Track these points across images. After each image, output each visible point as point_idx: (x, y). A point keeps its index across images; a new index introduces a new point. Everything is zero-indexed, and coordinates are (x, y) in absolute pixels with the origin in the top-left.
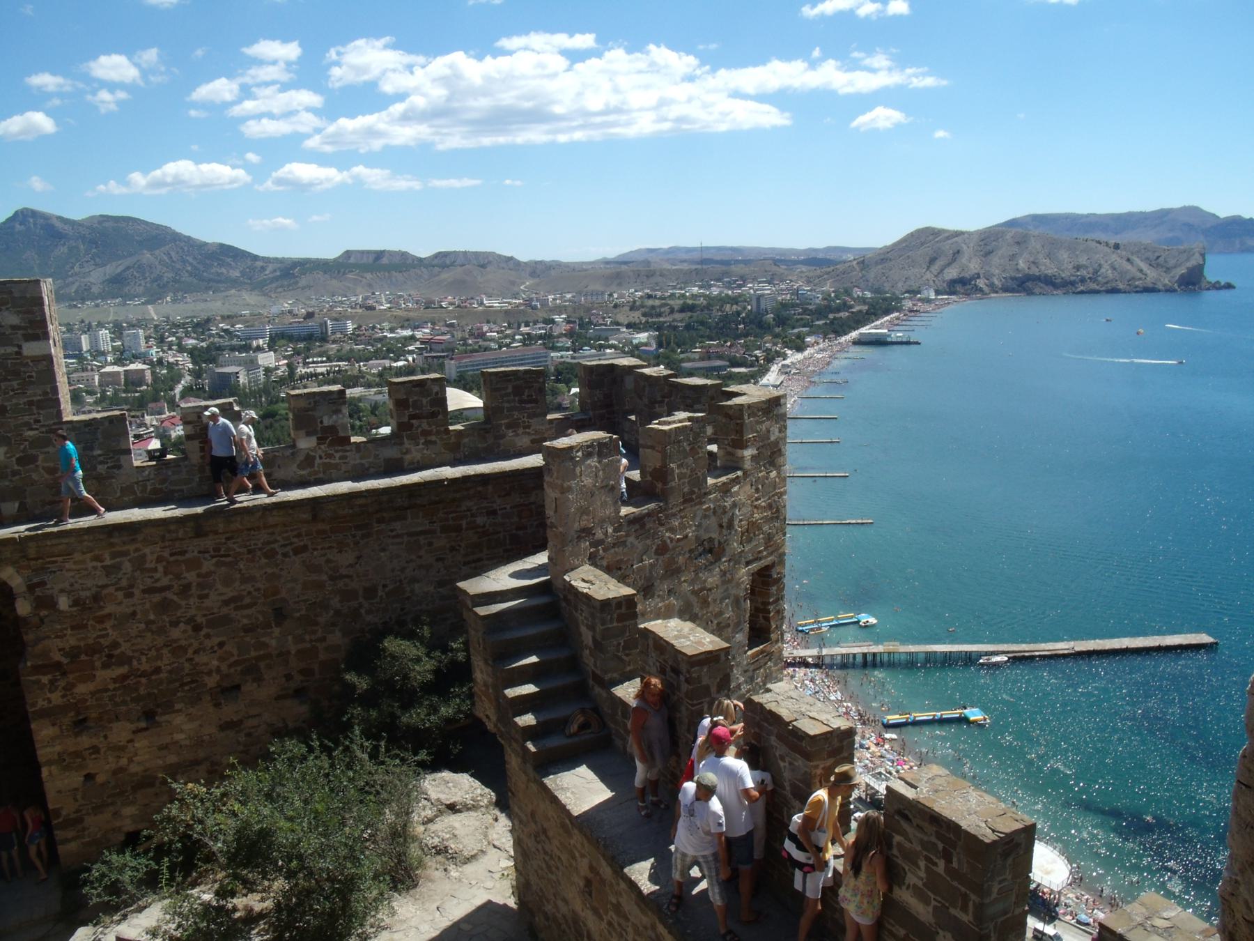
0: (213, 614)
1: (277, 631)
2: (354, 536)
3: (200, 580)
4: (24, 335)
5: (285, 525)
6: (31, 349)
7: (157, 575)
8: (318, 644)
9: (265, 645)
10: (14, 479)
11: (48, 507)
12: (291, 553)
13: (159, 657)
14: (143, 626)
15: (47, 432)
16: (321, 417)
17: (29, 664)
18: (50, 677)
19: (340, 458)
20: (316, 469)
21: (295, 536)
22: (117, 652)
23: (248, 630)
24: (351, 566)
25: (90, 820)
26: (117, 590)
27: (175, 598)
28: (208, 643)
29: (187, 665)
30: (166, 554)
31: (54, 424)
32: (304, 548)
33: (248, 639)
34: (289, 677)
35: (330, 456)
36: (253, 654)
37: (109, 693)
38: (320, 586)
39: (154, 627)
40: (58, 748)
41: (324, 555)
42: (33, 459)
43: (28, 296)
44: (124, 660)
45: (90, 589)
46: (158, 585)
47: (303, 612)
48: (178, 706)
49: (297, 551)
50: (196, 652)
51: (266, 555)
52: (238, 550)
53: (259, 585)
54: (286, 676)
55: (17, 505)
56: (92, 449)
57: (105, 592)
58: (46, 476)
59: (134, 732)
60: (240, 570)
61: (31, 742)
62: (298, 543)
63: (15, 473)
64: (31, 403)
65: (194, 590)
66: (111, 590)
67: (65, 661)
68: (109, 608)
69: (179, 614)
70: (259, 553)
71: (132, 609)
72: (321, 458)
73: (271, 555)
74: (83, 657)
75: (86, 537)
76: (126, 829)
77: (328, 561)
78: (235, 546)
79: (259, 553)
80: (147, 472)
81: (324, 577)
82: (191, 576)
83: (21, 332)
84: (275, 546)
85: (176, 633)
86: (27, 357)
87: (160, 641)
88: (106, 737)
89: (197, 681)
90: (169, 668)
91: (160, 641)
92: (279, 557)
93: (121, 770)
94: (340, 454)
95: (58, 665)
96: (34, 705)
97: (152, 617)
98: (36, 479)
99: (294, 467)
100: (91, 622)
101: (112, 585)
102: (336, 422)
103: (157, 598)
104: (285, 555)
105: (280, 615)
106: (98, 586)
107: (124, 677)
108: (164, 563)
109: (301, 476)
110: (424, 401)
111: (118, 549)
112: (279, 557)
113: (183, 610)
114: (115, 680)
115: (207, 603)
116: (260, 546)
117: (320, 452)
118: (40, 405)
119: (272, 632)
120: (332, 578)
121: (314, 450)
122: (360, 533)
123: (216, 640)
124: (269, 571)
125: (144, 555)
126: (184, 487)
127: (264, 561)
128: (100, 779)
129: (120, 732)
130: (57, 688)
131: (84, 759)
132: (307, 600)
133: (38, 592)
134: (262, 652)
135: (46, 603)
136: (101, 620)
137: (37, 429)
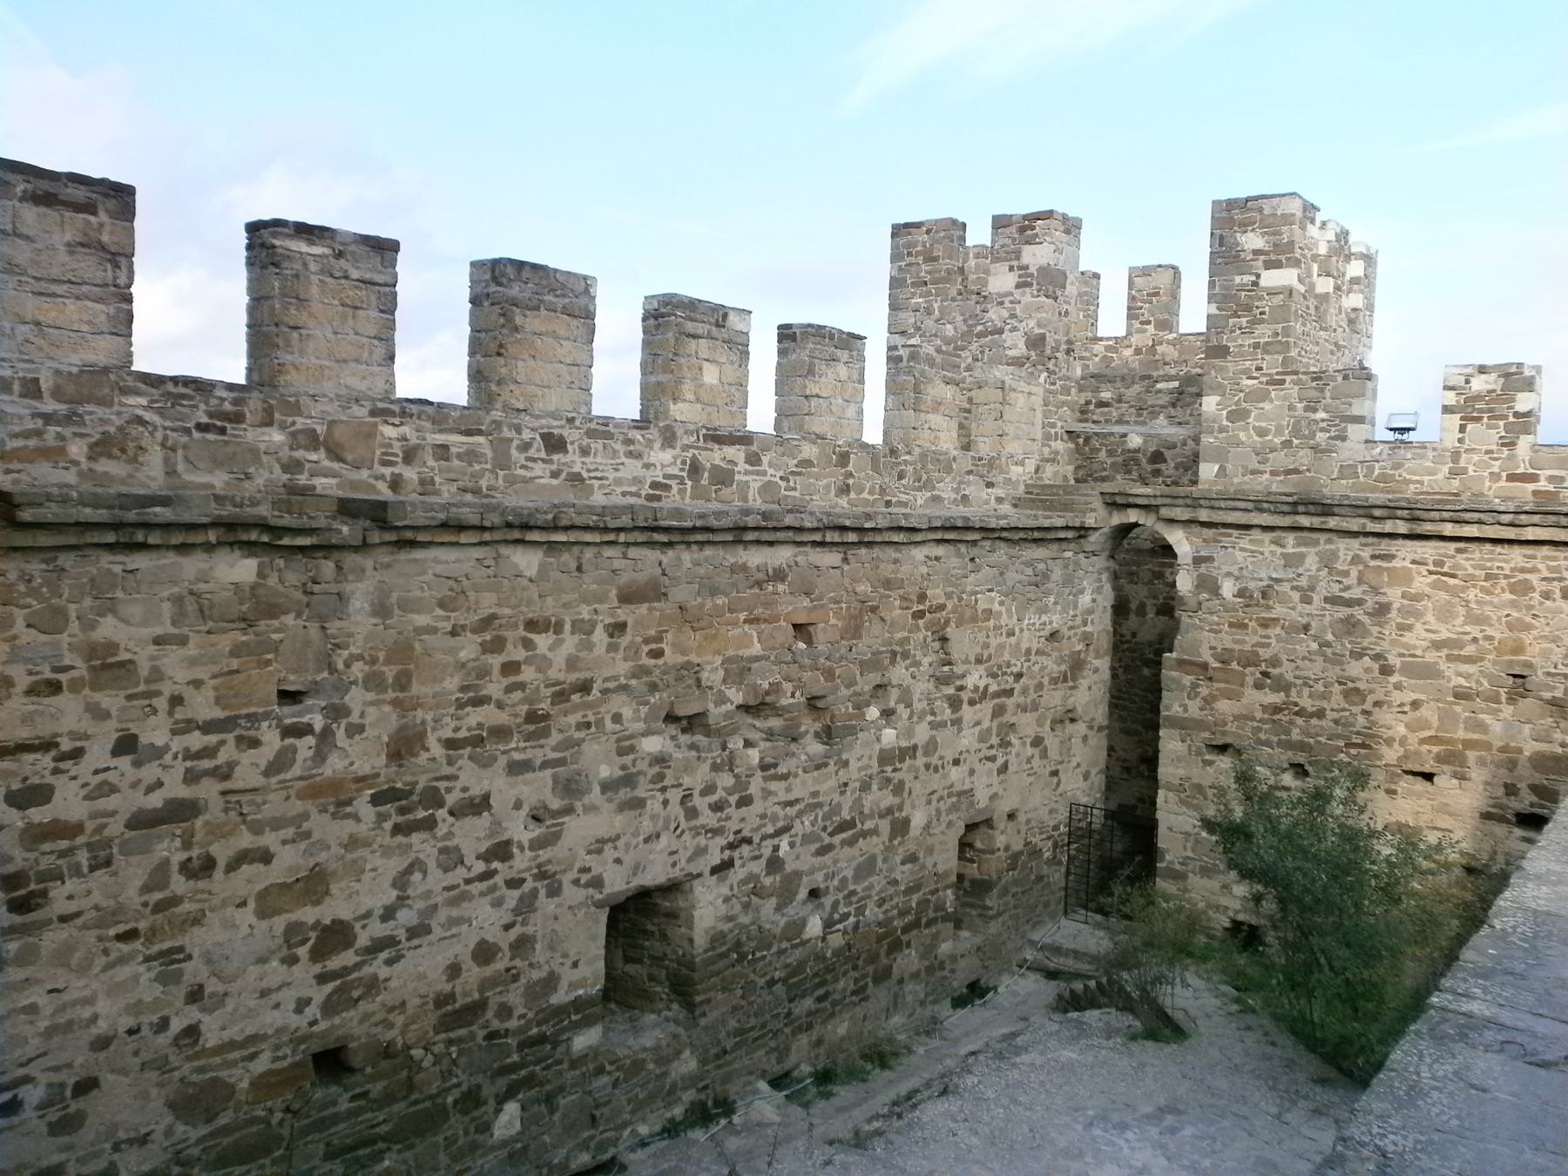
0: (1413, 656)
1: (1507, 711)
3: (1406, 602)
6: (1271, 278)
7: (1346, 581)
9: (1482, 727)
13: (1324, 696)
14: (1314, 646)
18: (1192, 678)
22: (1274, 671)
23: (1460, 695)
25: (1194, 880)
26: (1293, 588)
27: (1366, 620)
28: (1397, 697)
29: (1361, 720)
34: (1511, 790)
36: (1461, 734)
39: (1329, 651)
40: (1181, 772)
44: (1282, 686)
46: (1346, 595)
50: (1377, 704)
52: (1471, 571)
53: (1490, 632)
54: (1506, 786)
55: (1216, 467)
56: (1315, 410)
61: (1157, 751)
63: (1222, 430)
64: (1256, 346)
65: (1393, 614)
66: (1286, 587)
68: (1279, 611)
69: (1365, 644)
71: (1304, 621)
73: (1522, 588)
74: (1234, 665)
78: (1467, 564)
79: (1503, 582)
85: (1355, 668)
87: (1333, 673)
90: (1335, 715)
91: (1333, 673)
92: (1536, 595)
95: (1204, 666)
96: (1168, 708)
97: (1330, 637)
103: (1344, 612)
104: (1547, 595)
106: (1271, 579)
107: (1277, 709)
112: (1536, 595)
114: (1264, 708)
115: (1408, 638)
118: (1267, 348)
123: (1410, 696)
127: (1508, 596)
130: (1197, 694)
131: (1206, 799)
133: (1203, 569)
134: (1476, 736)
135: (1208, 585)
136: (1265, 623)
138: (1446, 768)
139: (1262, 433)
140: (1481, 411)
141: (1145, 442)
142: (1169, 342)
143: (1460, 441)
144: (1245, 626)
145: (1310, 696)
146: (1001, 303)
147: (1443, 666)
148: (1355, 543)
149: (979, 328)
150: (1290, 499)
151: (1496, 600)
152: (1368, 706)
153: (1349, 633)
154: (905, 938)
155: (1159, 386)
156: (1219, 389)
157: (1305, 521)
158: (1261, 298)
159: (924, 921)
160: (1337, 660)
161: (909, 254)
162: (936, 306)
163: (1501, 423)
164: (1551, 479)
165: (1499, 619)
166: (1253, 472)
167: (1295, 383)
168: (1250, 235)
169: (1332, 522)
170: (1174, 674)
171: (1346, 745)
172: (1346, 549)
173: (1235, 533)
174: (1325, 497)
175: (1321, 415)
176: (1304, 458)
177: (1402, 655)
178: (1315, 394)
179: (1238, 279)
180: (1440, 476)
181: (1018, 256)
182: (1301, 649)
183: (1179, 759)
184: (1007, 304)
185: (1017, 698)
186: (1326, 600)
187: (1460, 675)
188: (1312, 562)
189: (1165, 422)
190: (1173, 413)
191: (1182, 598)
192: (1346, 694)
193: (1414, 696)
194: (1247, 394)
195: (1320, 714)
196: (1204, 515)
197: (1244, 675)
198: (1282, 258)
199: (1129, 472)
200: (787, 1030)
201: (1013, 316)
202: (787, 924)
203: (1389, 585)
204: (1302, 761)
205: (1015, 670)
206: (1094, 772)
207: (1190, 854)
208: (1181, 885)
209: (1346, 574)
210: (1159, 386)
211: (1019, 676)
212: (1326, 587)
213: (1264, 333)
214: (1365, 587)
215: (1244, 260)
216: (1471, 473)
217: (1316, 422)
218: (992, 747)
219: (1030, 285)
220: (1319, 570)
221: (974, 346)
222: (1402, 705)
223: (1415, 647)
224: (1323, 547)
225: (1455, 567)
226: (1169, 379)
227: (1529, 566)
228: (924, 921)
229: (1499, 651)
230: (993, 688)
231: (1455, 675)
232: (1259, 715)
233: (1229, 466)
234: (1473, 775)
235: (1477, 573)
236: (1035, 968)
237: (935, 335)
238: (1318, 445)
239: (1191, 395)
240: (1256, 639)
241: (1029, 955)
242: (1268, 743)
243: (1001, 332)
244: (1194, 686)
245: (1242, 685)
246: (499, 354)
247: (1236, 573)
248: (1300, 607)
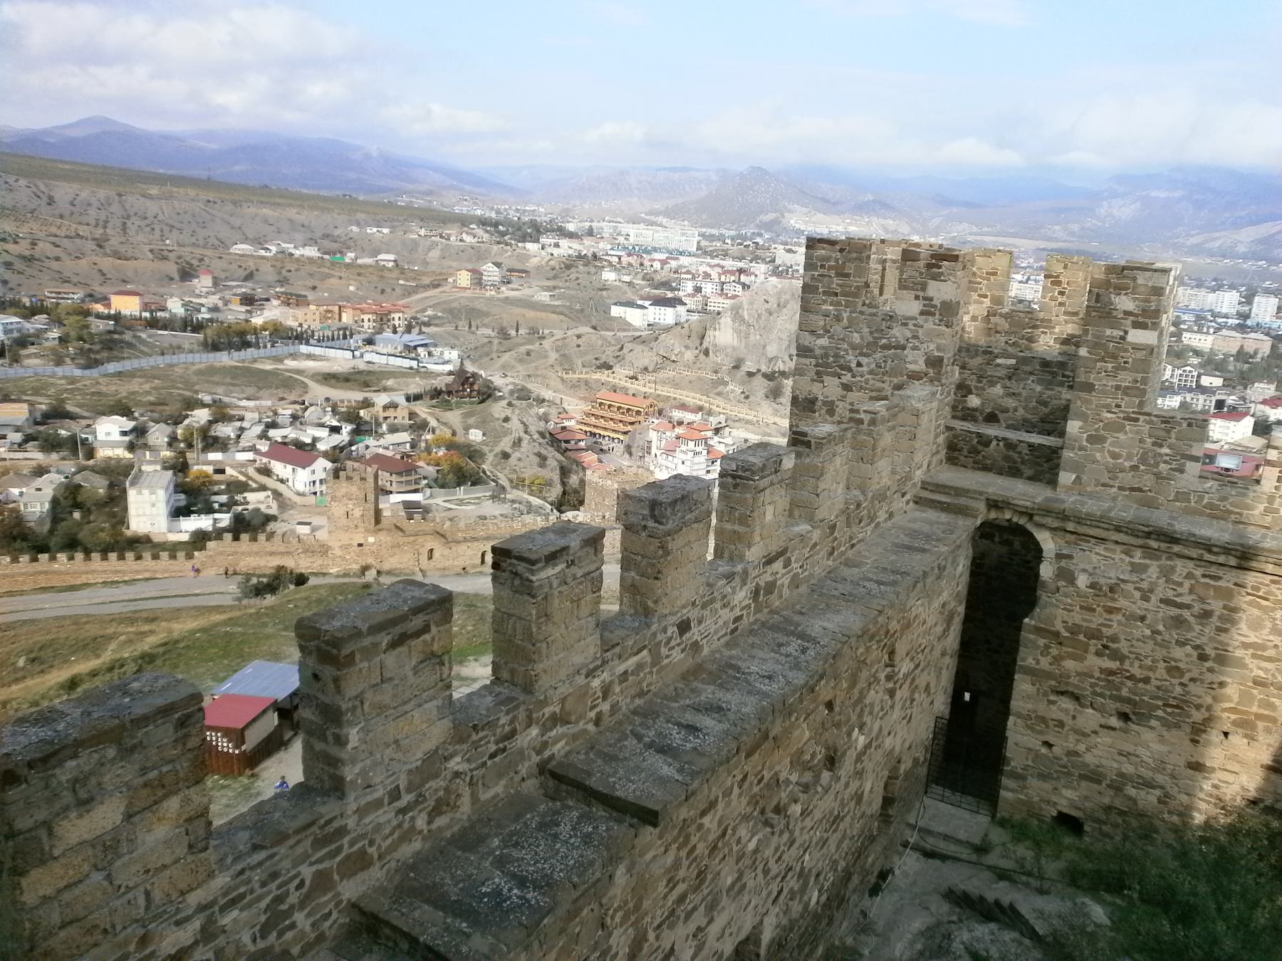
4: (1133, 322)
6: (1137, 336)
7: (1180, 590)
14: (1148, 632)
23: (1258, 683)
25: (1033, 782)
26: (1136, 589)
27: (1192, 619)
29: (1178, 689)
33: (1255, 692)
36: (1255, 709)
39: (1159, 638)
40: (1030, 706)
44: (1117, 656)
46: (1178, 600)
50: (1192, 680)
55: (1074, 476)
56: (1161, 446)
60: (1275, 619)
63: (1081, 449)
64: (1118, 388)
65: (1214, 619)
66: (1130, 587)
68: (1122, 603)
71: (1142, 613)
74: (1081, 637)
76: (1060, 808)
85: (1178, 653)
86: (1130, 344)
89: (1182, 708)
90: (1159, 683)
93: (1076, 754)
95: (1057, 634)
96: (1024, 660)
97: (1161, 628)
103: (1174, 611)
107: (1111, 672)
114: (1102, 671)
129: (1090, 718)
130: (1048, 653)
131: (1047, 727)
133: (1063, 563)
134: (1266, 712)
135: (1066, 576)
136: (1110, 611)
138: (1240, 730)
139: (1115, 456)
141: (983, 404)
142: (1001, 315)
144: (1094, 610)
145: (1140, 667)
146: (905, 325)
147: (1248, 660)
148: (1191, 564)
149: (884, 341)
150: (1146, 529)
152: (1184, 680)
153: (1177, 627)
155: (999, 361)
156: (1083, 417)
157: (1154, 544)
158: (1126, 350)
160: (1165, 645)
161: (822, 266)
162: (845, 315)
166: (1103, 485)
167: (1148, 422)
169: (1176, 548)
170: (1032, 636)
171: (1164, 705)
172: (1181, 567)
173: (1093, 541)
174: (1175, 532)
175: (1165, 450)
176: (1147, 481)
177: (1216, 649)
178: (1162, 433)
179: (1108, 332)
181: (924, 288)
183: (1029, 697)
184: (911, 327)
186: (1162, 601)
188: (1153, 571)
190: (1008, 384)
191: (1044, 582)
192: (1170, 670)
194: (1106, 425)
195: (1146, 680)
196: (1070, 526)
197: (1088, 645)
198: (1149, 321)
201: (915, 337)
203: (1214, 598)
204: (1128, 711)
207: (1030, 763)
208: (1021, 783)
210: (999, 361)
212: (1162, 591)
213: (1125, 379)
214: (1194, 597)
215: (1115, 317)
217: (1161, 455)
219: (933, 314)
220: (1158, 578)
221: (878, 355)
224: (1164, 562)
225: (1268, 593)
226: (1009, 356)
232: (1097, 674)
233: (1085, 478)
236: (915, 848)
237: (843, 340)
239: (1026, 372)
240: (1101, 621)
241: (913, 838)
242: (1102, 695)
243: (904, 348)
244: (1047, 647)
245: (1086, 652)
246: (657, 578)
247: (1090, 570)
248: (1140, 603)
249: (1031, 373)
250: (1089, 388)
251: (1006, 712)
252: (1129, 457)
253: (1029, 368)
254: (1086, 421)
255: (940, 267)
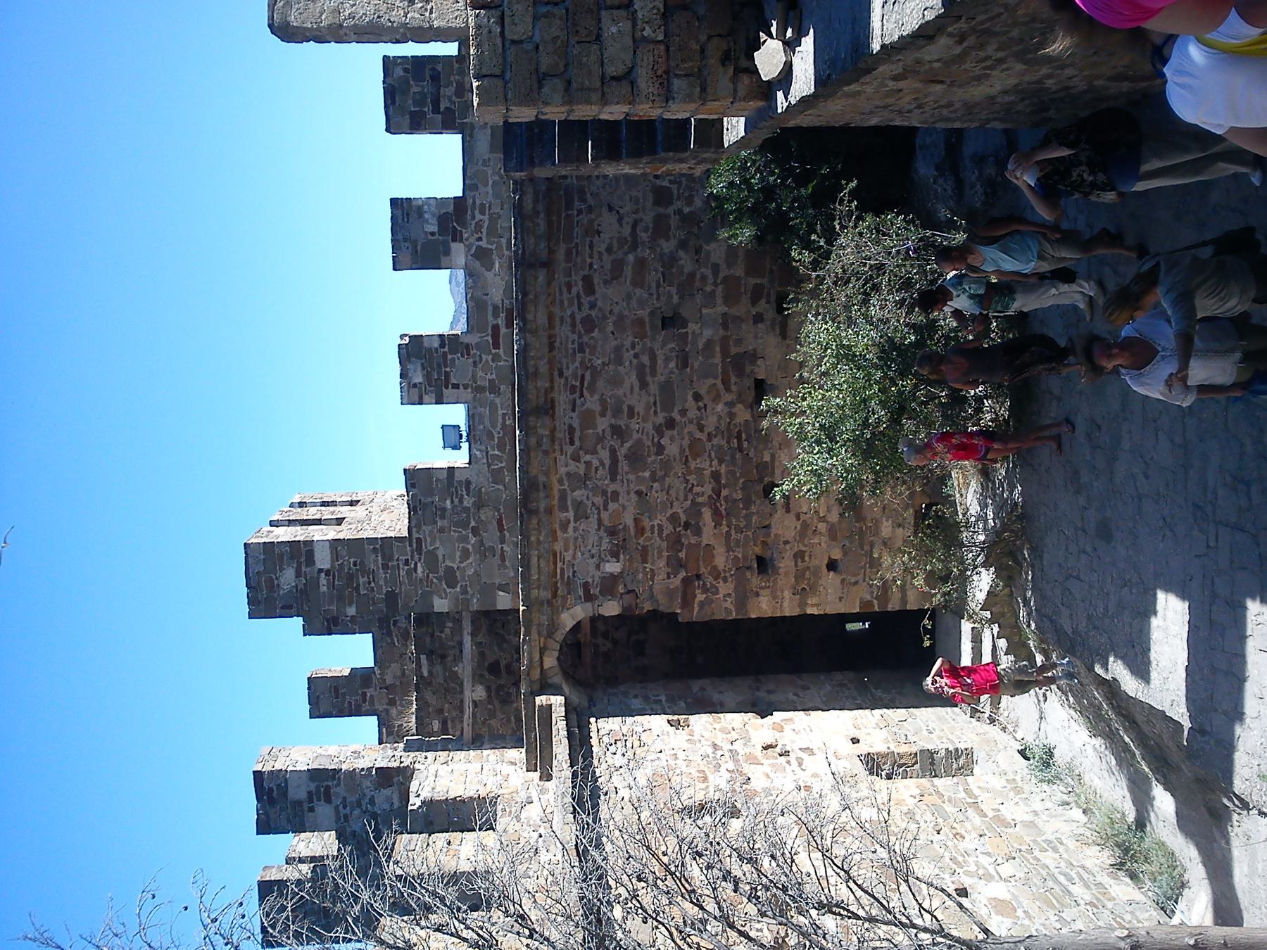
0: (655, 403)
1: (692, 327)
2: (580, 212)
3: (609, 413)
5: (553, 302)
6: (323, 560)
8: (721, 275)
9: (709, 344)
10: (470, 592)
11: (507, 563)
12: (592, 298)
13: (699, 471)
14: (656, 485)
15: (421, 554)
16: (426, 232)
17: (679, 611)
19: (482, 213)
20: (494, 247)
21: (569, 292)
23: (684, 362)
24: (620, 220)
26: (606, 509)
27: (627, 445)
28: (692, 414)
29: (715, 441)
30: (570, 450)
31: (411, 545)
32: (588, 281)
34: (758, 319)
35: (479, 226)
36: (717, 360)
37: (733, 532)
38: (641, 264)
39: (660, 474)
40: (787, 594)
41: (600, 253)
42: (450, 573)
43: (262, 557)
44: (695, 509)
45: (601, 538)
46: (607, 462)
47: (674, 290)
48: (767, 458)
49: (589, 288)
50: (701, 428)
51: (589, 330)
52: (577, 364)
53: (628, 343)
54: (755, 322)
56: (444, 510)
57: (606, 522)
58: (470, 561)
59: (788, 511)
60: (603, 363)
61: (773, 620)
62: (578, 287)
63: (464, 591)
64: (385, 567)
66: (605, 515)
67: (683, 574)
68: (628, 519)
69: (649, 443)
70: (585, 339)
71: (633, 495)
72: (480, 239)
73: (589, 324)
74: (682, 555)
75: (533, 538)
77: (609, 250)
78: (572, 367)
80: (478, 453)
81: (631, 257)
82: (603, 424)
83: (303, 569)
84: (578, 317)
85: (672, 449)
87: (679, 469)
88: (786, 542)
89: (739, 433)
90: (715, 462)
91: (679, 469)
92: (593, 313)
94: (477, 212)
95: (686, 582)
97: (647, 474)
98: (473, 570)
99: (489, 275)
100: (641, 541)
101: (599, 514)
102: (433, 215)
103: (624, 466)
104: (593, 306)
105: (671, 321)
106: (599, 529)
107: (717, 514)
108: (581, 452)
109: (501, 266)
110: (415, 89)
111: (556, 502)
112: (593, 313)
113: (644, 437)
114: (717, 524)
115: (639, 408)
116: (575, 337)
117: (472, 240)
118: (388, 557)
119: (693, 332)
120: (634, 247)
121: (469, 247)
122: (577, 203)
124: (610, 327)
125: (568, 474)
126: (500, 412)
127: (595, 334)
128: (837, 554)
132: (658, 286)
134: (718, 349)
135: (609, 585)
136: (640, 531)
137: (416, 564)
138: (748, 368)
139: (466, 554)
140: (439, 373)
143: (466, 387)
146: (346, 817)
151: (600, 343)
152: (703, 437)
154: (990, 814)
155: (426, 674)
156: (427, 596)
159: (969, 800)
160: (666, 465)
163: (450, 357)
164: (496, 315)
165: (616, 339)
168: (282, 580)
170: (696, 609)
177: (655, 412)
180: (498, 401)
181: (299, 803)
182: (662, 497)
183: (774, 597)
185: (738, 746)
187: (666, 367)
189: (461, 665)
191: (624, 609)
192: (696, 456)
193: (690, 398)
195: (716, 476)
199: (509, 694)
200: (1110, 905)
201: (359, 804)
202: (997, 913)
205: (710, 751)
206: (800, 682)
209: (588, 464)
210: (426, 674)
211: (715, 746)
216: (494, 376)
217: (454, 507)
218: (788, 762)
219: (328, 788)
222: (699, 409)
223: (648, 402)
225: (575, 376)
227: (569, 320)
228: (969, 800)
229: (643, 336)
230: (731, 766)
231: (667, 368)
233: (497, 581)
234: (751, 348)
235: (578, 360)
238: (474, 503)
249: (432, 635)
250: (392, 597)
251: (805, 617)
252: (465, 539)
253: (428, 640)
254: (430, 594)
255: (271, 790)
